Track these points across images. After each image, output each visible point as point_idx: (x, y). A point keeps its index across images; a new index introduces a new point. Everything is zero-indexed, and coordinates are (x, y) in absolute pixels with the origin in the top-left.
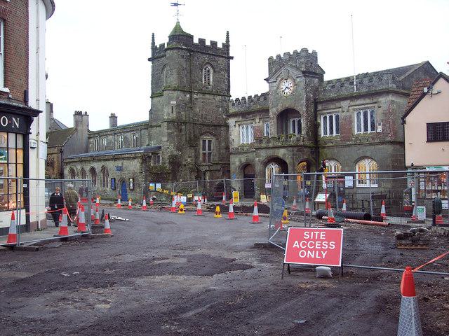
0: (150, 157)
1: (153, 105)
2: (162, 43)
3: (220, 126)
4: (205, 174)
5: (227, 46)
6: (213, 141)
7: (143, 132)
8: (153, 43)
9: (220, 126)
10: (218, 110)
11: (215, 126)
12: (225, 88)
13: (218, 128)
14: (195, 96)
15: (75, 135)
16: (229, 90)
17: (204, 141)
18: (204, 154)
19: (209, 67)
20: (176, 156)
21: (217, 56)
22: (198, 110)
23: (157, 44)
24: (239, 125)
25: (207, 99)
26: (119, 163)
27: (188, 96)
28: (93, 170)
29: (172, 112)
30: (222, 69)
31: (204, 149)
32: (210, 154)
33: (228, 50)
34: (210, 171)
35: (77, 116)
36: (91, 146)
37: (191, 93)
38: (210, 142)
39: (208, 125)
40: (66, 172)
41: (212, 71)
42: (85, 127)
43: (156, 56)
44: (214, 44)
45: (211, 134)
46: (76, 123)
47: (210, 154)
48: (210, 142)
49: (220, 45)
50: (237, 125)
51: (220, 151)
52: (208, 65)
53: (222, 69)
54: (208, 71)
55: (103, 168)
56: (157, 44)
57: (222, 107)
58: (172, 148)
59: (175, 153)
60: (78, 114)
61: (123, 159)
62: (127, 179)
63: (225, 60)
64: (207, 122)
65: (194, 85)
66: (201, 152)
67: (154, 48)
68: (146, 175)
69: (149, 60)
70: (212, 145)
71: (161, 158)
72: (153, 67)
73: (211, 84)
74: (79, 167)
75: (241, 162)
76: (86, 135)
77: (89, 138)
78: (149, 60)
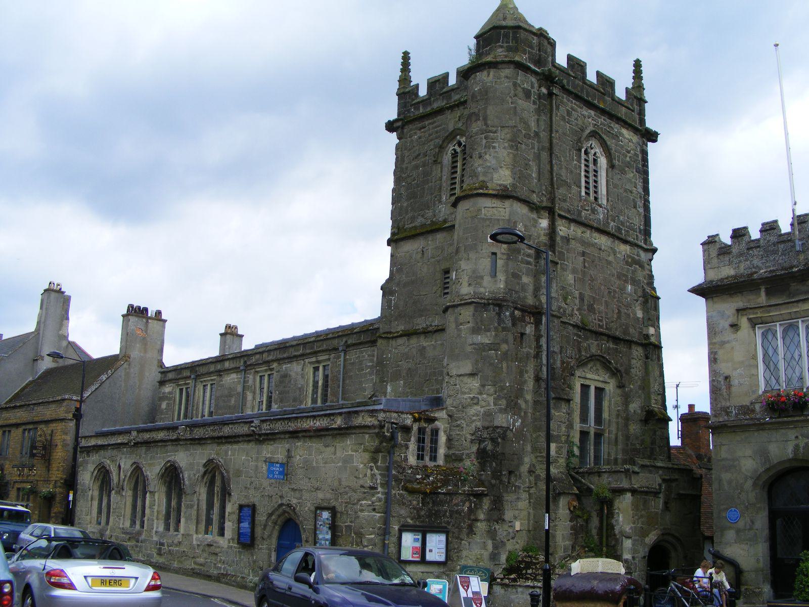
0: (407, 430)
1: (394, 260)
2: (437, 72)
3: (629, 343)
4: (610, 503)
5: (637, 96)
6: (611, 387)
7: (353, 356)
8: (405, 79)
9: (629, 343)
10: (623, 289)
11: (616, 339)
12: (638, 222)
13: (622, 348)
14: (563, 229)
15: (121, 372)
16: (647, 233)
17: (585, 388)
18: (584, 434)
19: (598, 150)
20: (504, 432)
21: (618, 120)
22: (570, 278)
23: (420, 79)
24: (753, 323)
25: (594, 245)
26: (277, 451)
27: (544, 223)
28: (172, 475)
29: (495, 276)
30: (628, 165)
31: (584, 418)
32: (598, 436)
33: (642, 113)
34: (634, 491)
35: (133, 319)
36: (164, 405)
37: (551, 212)
38: (599, 391)
39: (597, 334)
40: (86, 477)
41: (603, 161)
42: (152, 354)
43: (414, 112)
44: (606, 83)
45: (606, 365)
46: (127, 338)
47: (598, 436)
48: (599, 391)
49: (621, 94)
50: (744, 322)
51: (626, 425)
52: (593, 142)
53: (628, 165)
54: (595, 162)
55: (212, 471)
56: (420, 79)
57: (634, 282)
58: (488, 401)
59: (501, 420)
60: (136, 312)
61: (294, 435)
62: (305, 508)
63: (635, 138)
64: (593, 321)
65: (561, 192)
66: (577, 426)
67: (406, 93)
68: (388, 500)
69: (390, 127)
70: (605, 404)
71: (442, 438)
72: (398, 148)
73: (604, 202)
74: (126, 463)
75: (763, 454)
76: (153, 375)
77: (162, 383)
78: (390, 127)
